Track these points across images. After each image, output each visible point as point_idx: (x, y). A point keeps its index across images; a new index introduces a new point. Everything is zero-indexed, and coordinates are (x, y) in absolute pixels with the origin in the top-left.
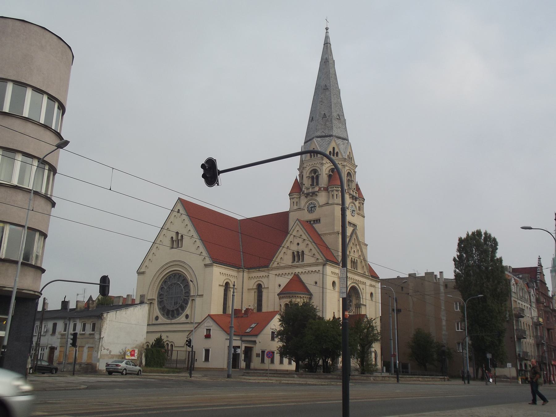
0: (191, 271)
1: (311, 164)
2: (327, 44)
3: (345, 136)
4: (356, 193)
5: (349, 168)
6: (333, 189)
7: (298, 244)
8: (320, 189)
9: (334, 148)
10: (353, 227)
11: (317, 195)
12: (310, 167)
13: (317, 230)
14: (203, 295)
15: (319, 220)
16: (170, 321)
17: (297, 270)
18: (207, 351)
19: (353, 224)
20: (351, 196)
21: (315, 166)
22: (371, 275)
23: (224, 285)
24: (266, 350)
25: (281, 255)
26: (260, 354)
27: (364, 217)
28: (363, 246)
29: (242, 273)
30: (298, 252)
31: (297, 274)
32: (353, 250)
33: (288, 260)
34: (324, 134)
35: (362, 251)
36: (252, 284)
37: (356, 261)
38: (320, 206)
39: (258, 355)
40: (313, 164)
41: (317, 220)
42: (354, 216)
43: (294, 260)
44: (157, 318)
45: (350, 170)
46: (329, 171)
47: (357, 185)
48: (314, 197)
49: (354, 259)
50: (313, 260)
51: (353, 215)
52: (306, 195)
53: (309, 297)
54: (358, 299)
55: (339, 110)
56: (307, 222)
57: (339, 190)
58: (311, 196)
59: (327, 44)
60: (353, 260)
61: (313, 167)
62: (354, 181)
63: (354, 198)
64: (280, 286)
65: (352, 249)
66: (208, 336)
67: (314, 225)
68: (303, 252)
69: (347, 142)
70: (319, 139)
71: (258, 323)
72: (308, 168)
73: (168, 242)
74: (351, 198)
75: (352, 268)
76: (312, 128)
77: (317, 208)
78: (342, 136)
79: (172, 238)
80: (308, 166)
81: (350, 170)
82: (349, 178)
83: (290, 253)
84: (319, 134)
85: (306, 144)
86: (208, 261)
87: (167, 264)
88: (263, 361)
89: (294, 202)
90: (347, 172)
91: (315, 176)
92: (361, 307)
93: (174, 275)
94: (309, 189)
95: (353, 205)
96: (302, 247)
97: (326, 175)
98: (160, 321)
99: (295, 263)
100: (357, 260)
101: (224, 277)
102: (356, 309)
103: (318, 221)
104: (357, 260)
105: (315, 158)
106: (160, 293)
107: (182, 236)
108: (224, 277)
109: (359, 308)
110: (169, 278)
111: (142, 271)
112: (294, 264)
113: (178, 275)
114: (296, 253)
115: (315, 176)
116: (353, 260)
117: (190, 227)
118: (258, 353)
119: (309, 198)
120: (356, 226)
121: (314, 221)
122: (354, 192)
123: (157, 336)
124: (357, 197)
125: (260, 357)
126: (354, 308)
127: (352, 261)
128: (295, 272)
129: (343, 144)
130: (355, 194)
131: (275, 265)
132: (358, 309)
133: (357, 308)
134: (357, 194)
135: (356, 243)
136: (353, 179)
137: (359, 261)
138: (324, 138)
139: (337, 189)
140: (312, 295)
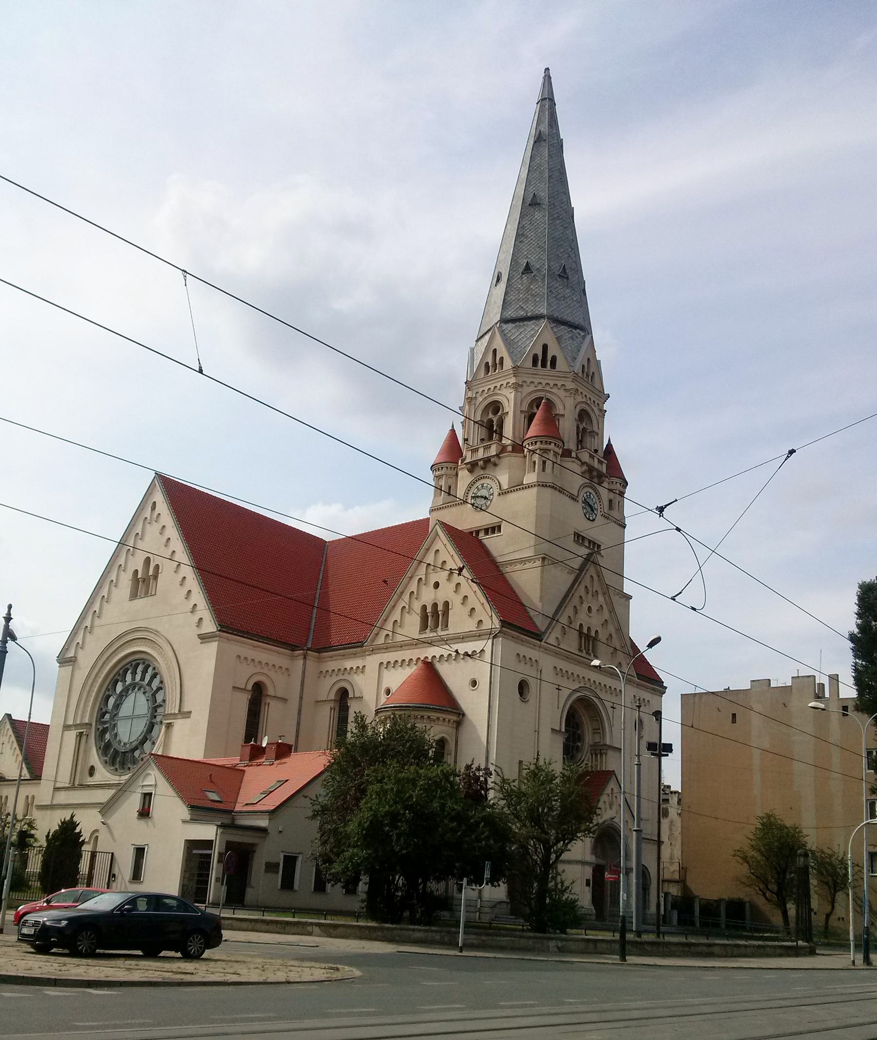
0: (171, 653)
2: (547, 102)
3: (577, 319)
4: (600, 462)
5: (584, 400)
7: (437, 585)
8: (503, 449)
9: (545, 348)
10: (588, 548)
11: (495, 465)
13: (494, 552)
14: (191, 712)
15: (499, 527)
16: (117, 778)
17: (431, 652)
18: (140, 852)
19: (590, 541)
20: (585, 468)
22: (637, 674)
23: (250, 687)
24: (299, 853)
25: (396, 615)
26: (278, 864)
27: (624, 526)
28: (615, 599)
29: (302, 661)
30: (435, 605)
31: (430, 661)
32: (585, 606)
33: (411, 627)
34: (522, 313)
35: (612, 611)
36: (327, 689)
37: (593, 634)
38: (503, 493)
39: (271, 867)
40: (492, 389)
42: (594, 520)
43: (424, 626)
44: (92, 771)
45: (587, 403)
46: (531, 405)
47: (609, 445)
48: (489, 472)
49: (589, 628)
50: (470, 626)
51: (591, 518)
52: (469, 466)
53: (455, 718)
54: (599, 731)
55: (566, 256)
56: (471, 533)
57: (550, 450)
58: (483, 468)
59: (547, 102)
60: (585, 631)
61: (490, 396)
62: (598, 434)
63: (595, 473)
64: (388, 691)
65: (585, 603)
66: (144, 813)
67: (485, 542)
68: (446, 604)
69: (582, 334)
70: (510, 326)
71: (287, 781)
72: (480, 399)
73: (126, 580)
74: (587, 476)
75: (580, 650)
76: (495, 303)
78: (569, 319)
79: (136, 571)
80: (481, 395)
81: (587, 403)
82: (584, 424)
83: (417, 607)
84: (510, 313)
85: (479, 343)
86: (210, 626)
87: (119, 637)
88: (288, 883)
90: (578, 409)
91: (495, 419)
92: (606, 754)
93: (134, 663)
94: (477, 450)
95: (594, 494)
96: (446, 592)
97: (523, 416)
98: (98, 778)
99: (429, 634)
100: (597, 631)
101: (251, 670)
102: (594, 756)
103: (495, 529)
104: (597, 631)
105: (497, 371)
106: (102, 709)
107: (157, 567)
108: (251, 670)
109: (601, 754)
110: (124, 671)
111: (71, 654)
112: (424, 636)
113: (144, 663)
114: (429, 610)
115: (495, 419)
116: (585, 631)
117: (178, 545)
118: (273, 860)
119: (479, 472)
120: (599, 546)
121: (487, 531)
122: (596, 460)
123: (66, 815)
124: (604, 471)
125: (278, 872)
126: (589, 755)
127: (580, 632)
128: (427, 657)
129: (572, 338)
130: (596, 464)
131: (381, 640)
132: (599, 756)
133: (596, 755)
134: (604, 466)
135: (597, 586)
136: (595, 429)
137: (602, 636)
138: (521, 324)
139: (545, 446)
140: (464, 715)
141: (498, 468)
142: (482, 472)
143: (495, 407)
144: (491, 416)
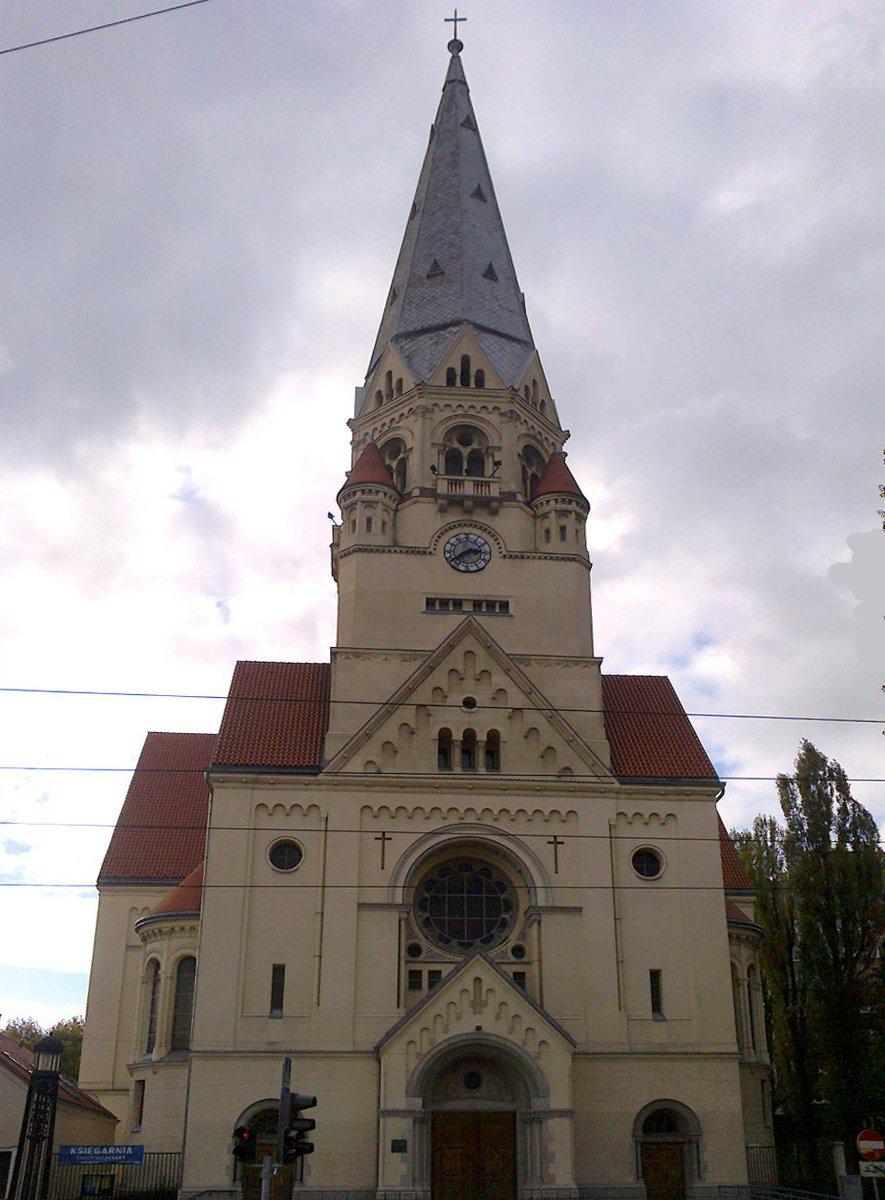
1: (455, 404)
6: (569, 507)
12: (448, 413)
15: (505, 606)
21: (483, 420)
38: (511, 556)
41: (491, 605)
48: (481, 517)
58: (469, 511)
61: (464, 416)
77: (496, 559)
89: (369, 521)
91: (465, 451)
115: (465, 451)
119: (454, 516)
121: (477, 604)
141: (497, 518)
142: (467, 517)
143: (465, 433)
144: (456, 445)
